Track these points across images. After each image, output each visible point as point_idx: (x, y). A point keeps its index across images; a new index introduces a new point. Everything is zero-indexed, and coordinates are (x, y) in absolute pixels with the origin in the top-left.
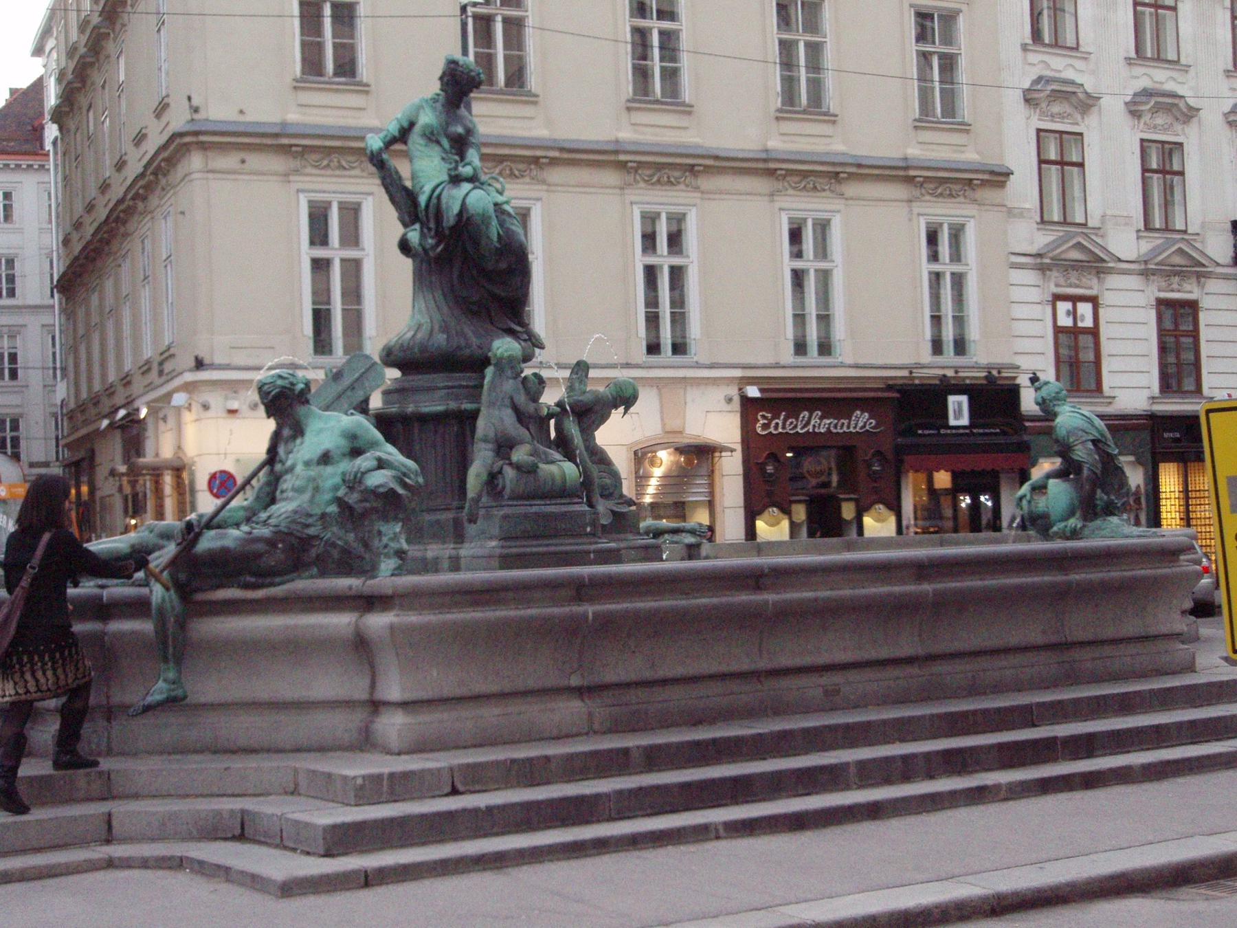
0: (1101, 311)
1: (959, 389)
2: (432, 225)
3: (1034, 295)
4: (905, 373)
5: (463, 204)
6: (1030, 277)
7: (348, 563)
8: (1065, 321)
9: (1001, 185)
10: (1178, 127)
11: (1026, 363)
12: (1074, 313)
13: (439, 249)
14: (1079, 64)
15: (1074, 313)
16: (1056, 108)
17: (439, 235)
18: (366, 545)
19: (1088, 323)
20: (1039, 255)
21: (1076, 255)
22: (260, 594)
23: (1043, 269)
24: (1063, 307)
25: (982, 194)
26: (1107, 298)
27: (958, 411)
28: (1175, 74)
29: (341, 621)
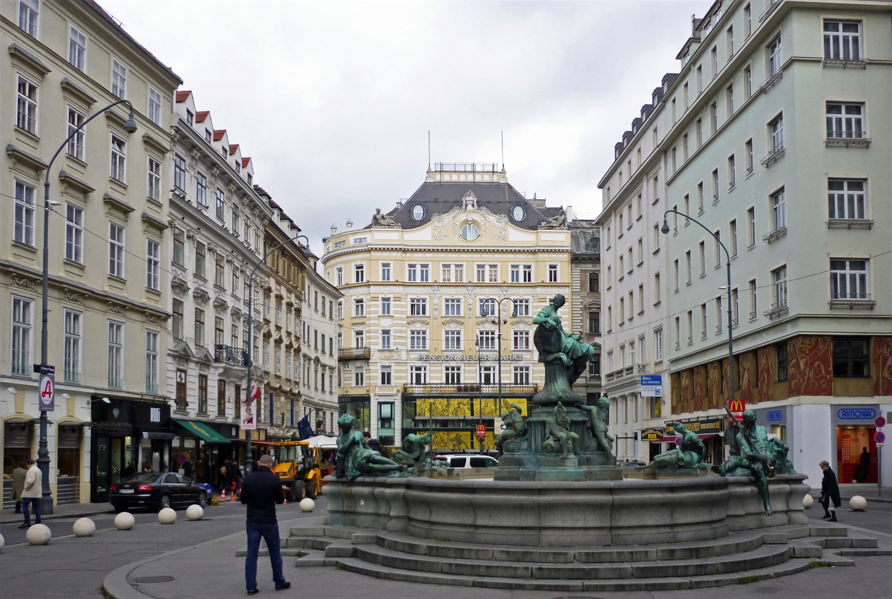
0: (188, 377)
1: (156, 406)
2: (570, 354)
3: (173, 367)
4: (140, 397)
5: (588, 349)
6: (170, 359)
7: (780, 471)
8: (179, 380)
9: (166, 320)
10: (203, 304)
11: (169, 395)
12: (180, 376)
13: (571, 363)
14: (183, 273)
15: (180, 376)
16: (177, 290)
17: (572, 359)
18: (784, 464)
19: (183, 381)
20: (176, 352)
21: (182, 353)
22: (773, 479)
23: (174, 357)
24: (179, 373)
25: (163, 323)
26: (189, 372)
27: (155, 415)
28: (203, 283)
29: (786, 487)
